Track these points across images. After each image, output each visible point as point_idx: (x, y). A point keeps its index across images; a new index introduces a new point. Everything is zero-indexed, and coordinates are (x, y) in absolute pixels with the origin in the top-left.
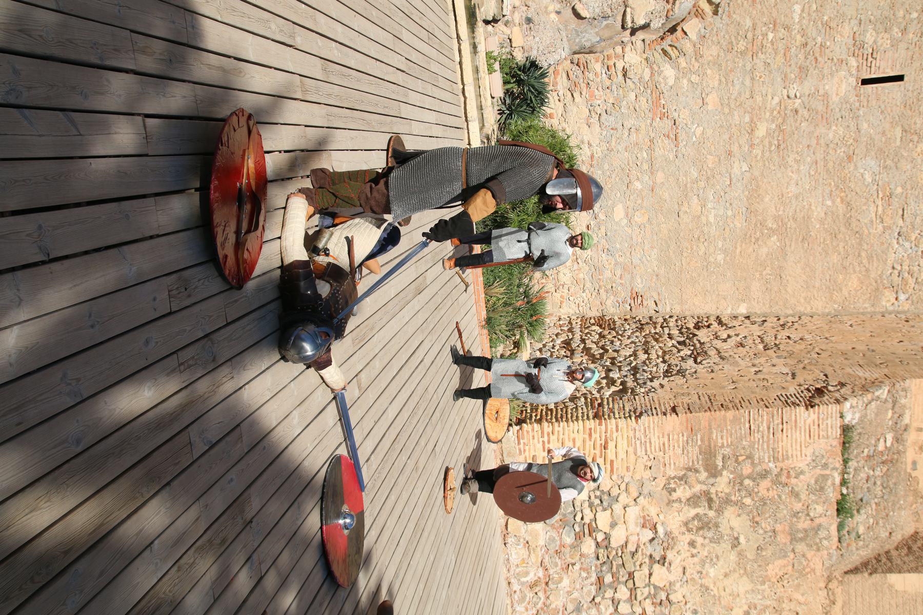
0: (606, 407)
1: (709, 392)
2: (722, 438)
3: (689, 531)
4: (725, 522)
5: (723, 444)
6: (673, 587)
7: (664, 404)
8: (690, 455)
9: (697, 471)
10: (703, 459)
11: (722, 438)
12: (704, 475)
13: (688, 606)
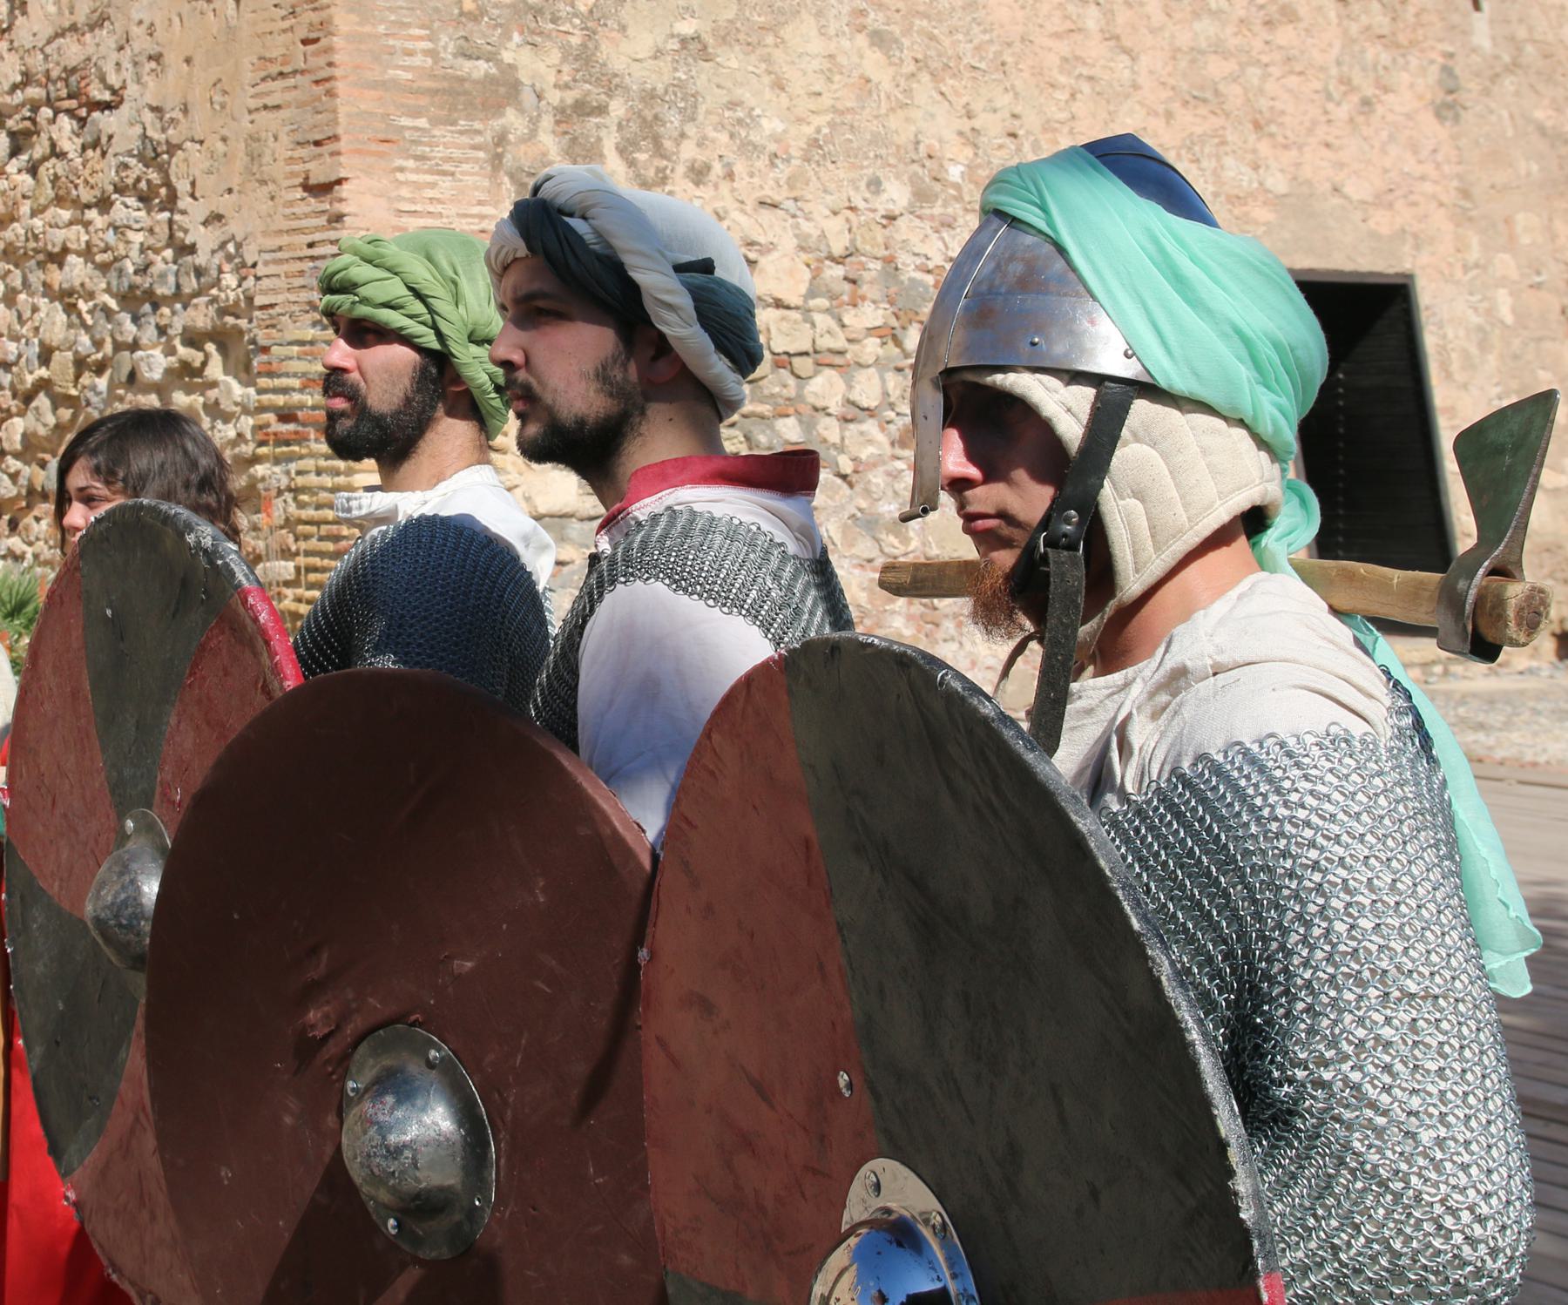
0: (296, 397)
1: (249, 77)
2: (410, 53)
3: (664, 180)
4: (638, 72)
5: (427, 53)
6: (812, 242)
7: (295, 217)
8: (457, 153)
9: (501, 139)
10: (469, 118)
11: (410, 53)
12: (512, 119)
13: (861, 205)
